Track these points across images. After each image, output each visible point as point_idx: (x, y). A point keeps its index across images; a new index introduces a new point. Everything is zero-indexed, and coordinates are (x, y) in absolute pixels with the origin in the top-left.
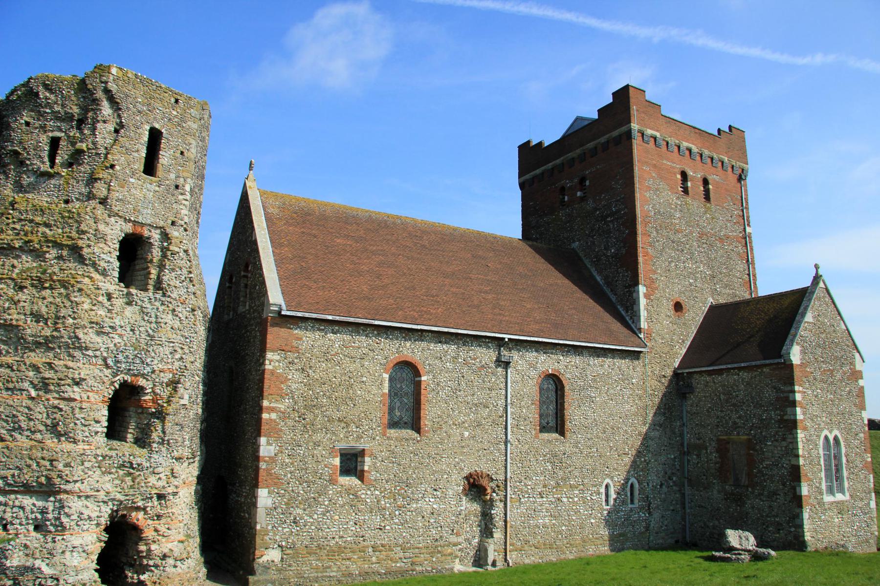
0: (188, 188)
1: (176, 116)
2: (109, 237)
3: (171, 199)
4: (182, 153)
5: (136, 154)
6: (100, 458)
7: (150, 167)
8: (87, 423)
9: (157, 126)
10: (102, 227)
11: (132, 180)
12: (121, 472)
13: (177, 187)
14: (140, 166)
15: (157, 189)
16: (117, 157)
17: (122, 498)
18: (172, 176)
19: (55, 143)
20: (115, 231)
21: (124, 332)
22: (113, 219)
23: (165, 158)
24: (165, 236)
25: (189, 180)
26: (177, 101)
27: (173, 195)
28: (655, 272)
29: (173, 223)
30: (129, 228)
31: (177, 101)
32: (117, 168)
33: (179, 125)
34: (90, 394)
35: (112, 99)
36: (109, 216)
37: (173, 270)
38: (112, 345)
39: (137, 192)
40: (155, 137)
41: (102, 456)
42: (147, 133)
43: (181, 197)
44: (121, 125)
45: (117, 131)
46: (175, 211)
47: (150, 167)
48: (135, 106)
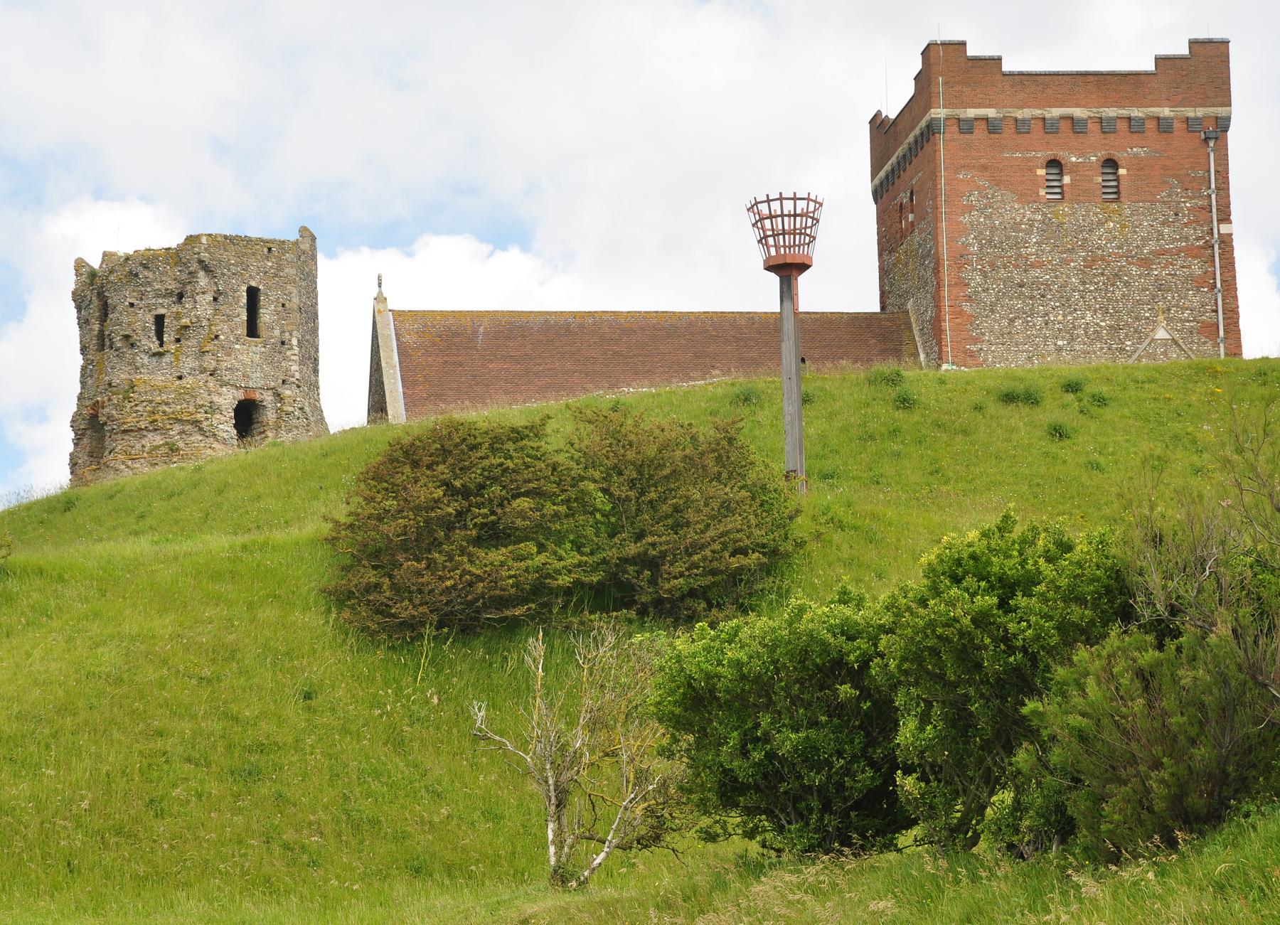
0: (294, 342)
2: (223, 408)
3: (278, 357)
4: (283, 305)
7: (252, 330)
9: (253, 284)
10: (216, 399)
11: (237, 347)
13: (283, 343)
14: (242, 330)
16: (222, 328)
18: (277, 332)
19: (159, 320)
20: (228, 399)
24: (278, 396)
25: (295, 333)
26: (270, 249)
28: (975, 341)
31: (270, 249)
32: (222, 337)
33: (276, 275)
35: (207, 269)
37: (290, 430)
39: (245, 358)
43: (289, 353)
44: (219, 292)
45: (215, 299)
47: (252, 330)
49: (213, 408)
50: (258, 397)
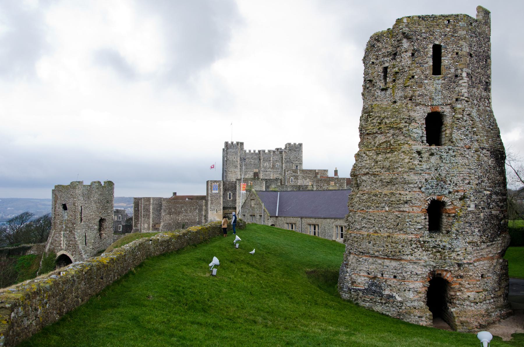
1: (449, 32)
2: (417, 119)
5: (426, 65)
6: (422, 242)
7: (437, 69)
8: (413, 224)
9: (437, 43)
12: (434, 250)
13: (456, 76)
15: (443, 81)
17: (434, 265)
18: (453, 70)
21: (430, 172)
22: (418, 107)
23: (446, 61)
27: (454, 82)
29: (457, 100)
30: (429, 110)
32: (416, 77)
33: (453, 36)
34: (414, 208)
36: (416, 106)
38: (424, 180)
40: (437, 49)
41: (423, 241)
42: (432, 49)
46: (457, 92)
47: (437, 69)
48: (421, 36)
49: (410, 120)
50: (440, 110)
